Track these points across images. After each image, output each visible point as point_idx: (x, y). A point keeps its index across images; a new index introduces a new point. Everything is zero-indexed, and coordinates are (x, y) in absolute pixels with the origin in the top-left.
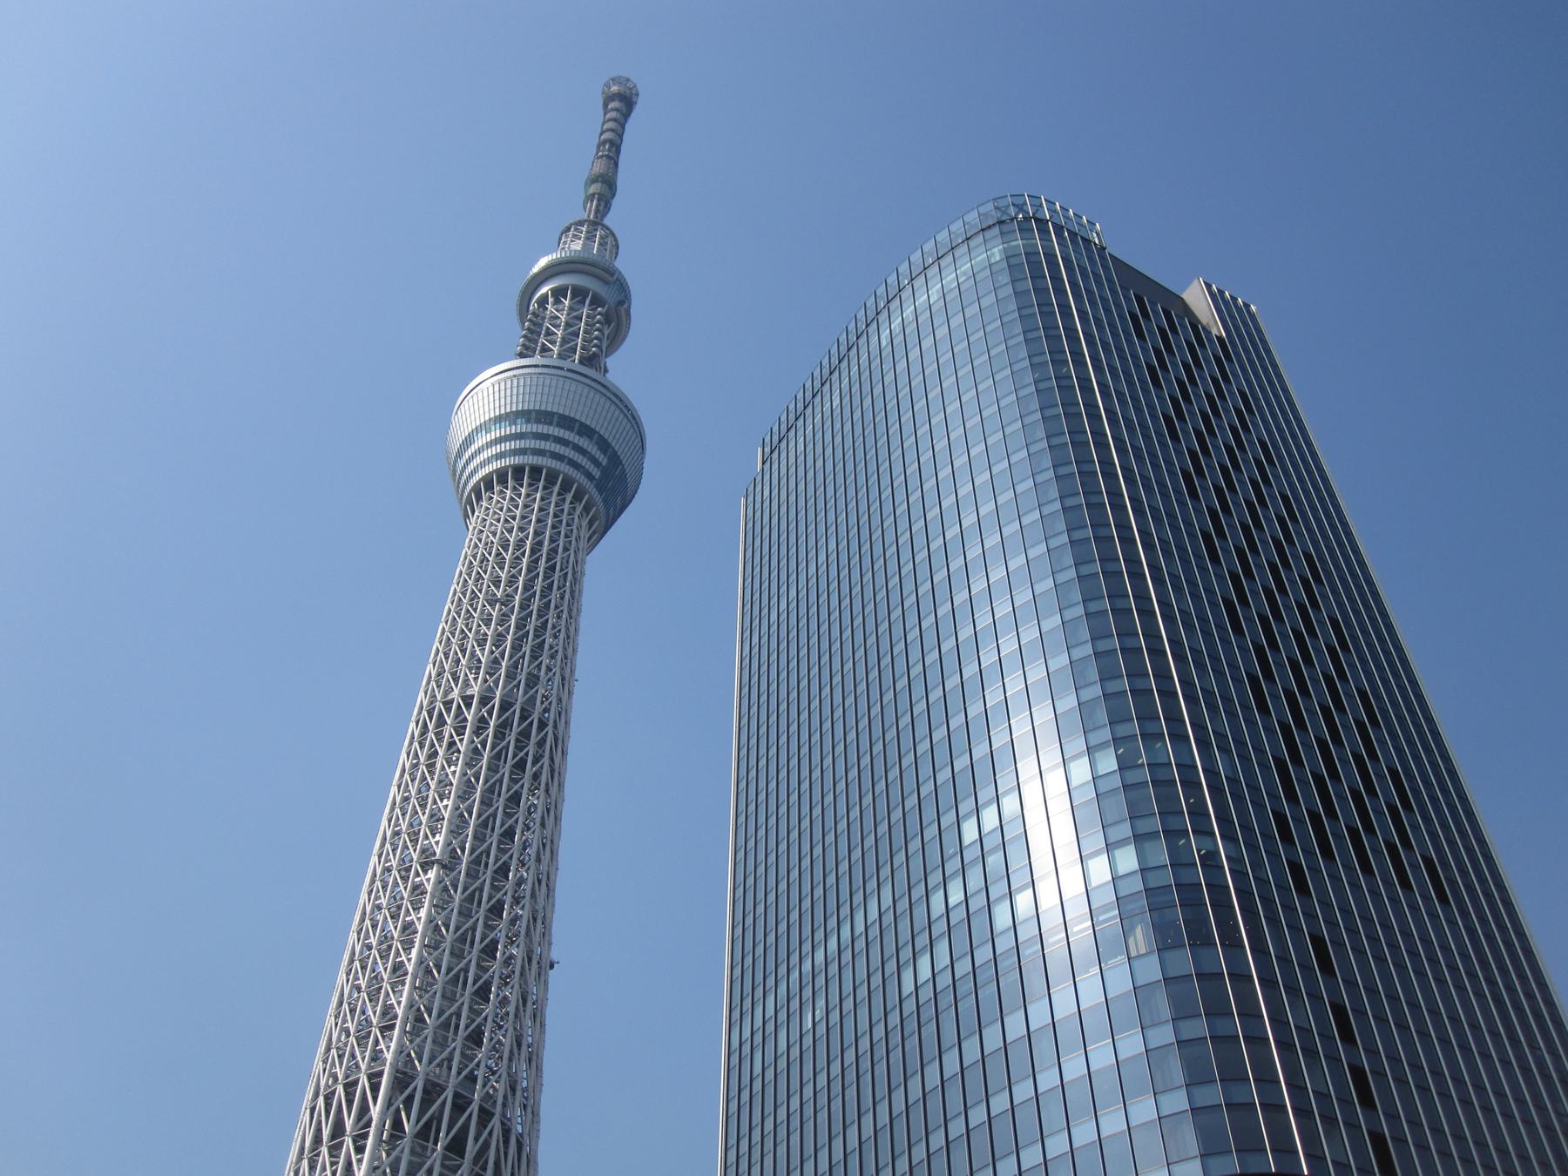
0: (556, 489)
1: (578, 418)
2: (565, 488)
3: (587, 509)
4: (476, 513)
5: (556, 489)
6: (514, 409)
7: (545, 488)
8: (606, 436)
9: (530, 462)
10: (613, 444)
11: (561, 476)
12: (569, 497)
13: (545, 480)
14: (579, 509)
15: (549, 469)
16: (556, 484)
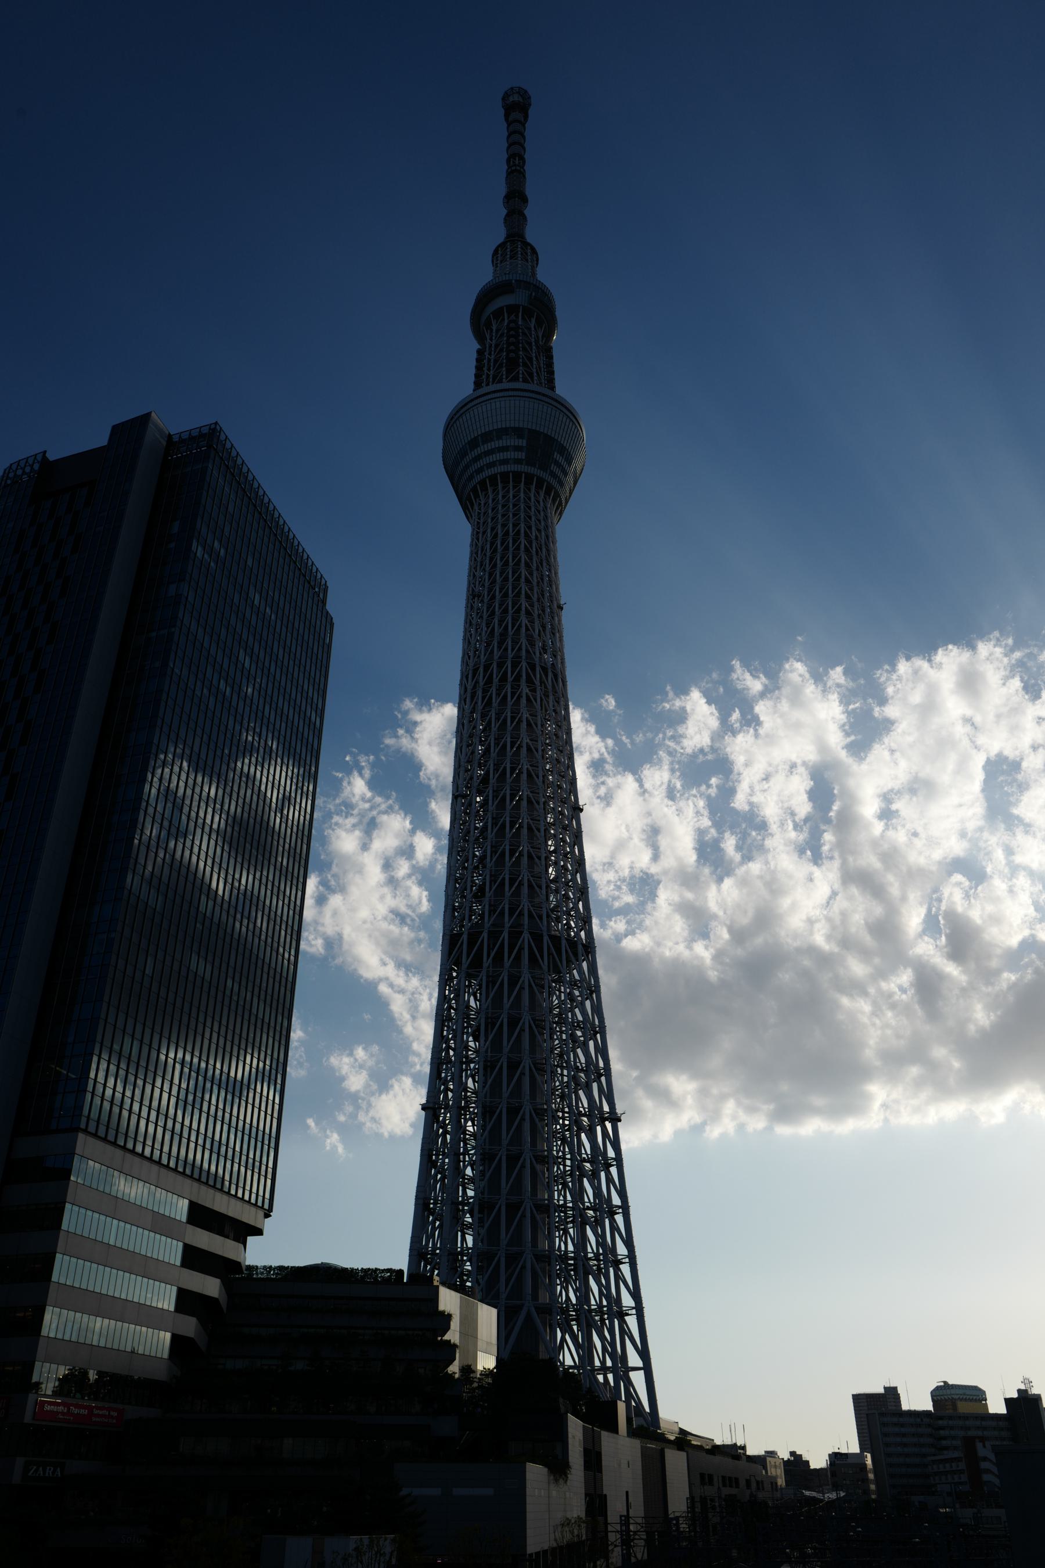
0: (522, 485)
1: (525, 426)
2: (528, 483)
3: (548, 493)
4: (473, 518)
5: (522, 485)
6: (480, 433)
7: (514, 487)
8: (549, 434)
9: (499, 471)
10: (556, 438)
11: (523, 475)
12: (533, 487)
13: (513, 481)
14: (542, 494)
15: (514, 472)
16: (521, 481)
